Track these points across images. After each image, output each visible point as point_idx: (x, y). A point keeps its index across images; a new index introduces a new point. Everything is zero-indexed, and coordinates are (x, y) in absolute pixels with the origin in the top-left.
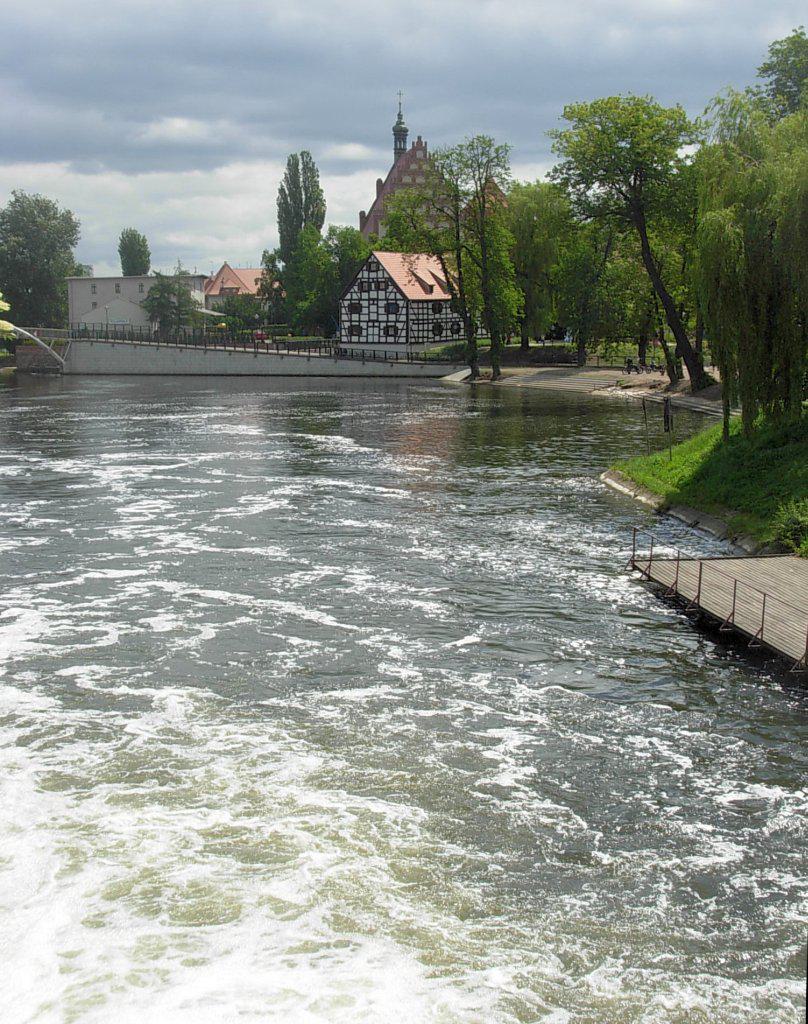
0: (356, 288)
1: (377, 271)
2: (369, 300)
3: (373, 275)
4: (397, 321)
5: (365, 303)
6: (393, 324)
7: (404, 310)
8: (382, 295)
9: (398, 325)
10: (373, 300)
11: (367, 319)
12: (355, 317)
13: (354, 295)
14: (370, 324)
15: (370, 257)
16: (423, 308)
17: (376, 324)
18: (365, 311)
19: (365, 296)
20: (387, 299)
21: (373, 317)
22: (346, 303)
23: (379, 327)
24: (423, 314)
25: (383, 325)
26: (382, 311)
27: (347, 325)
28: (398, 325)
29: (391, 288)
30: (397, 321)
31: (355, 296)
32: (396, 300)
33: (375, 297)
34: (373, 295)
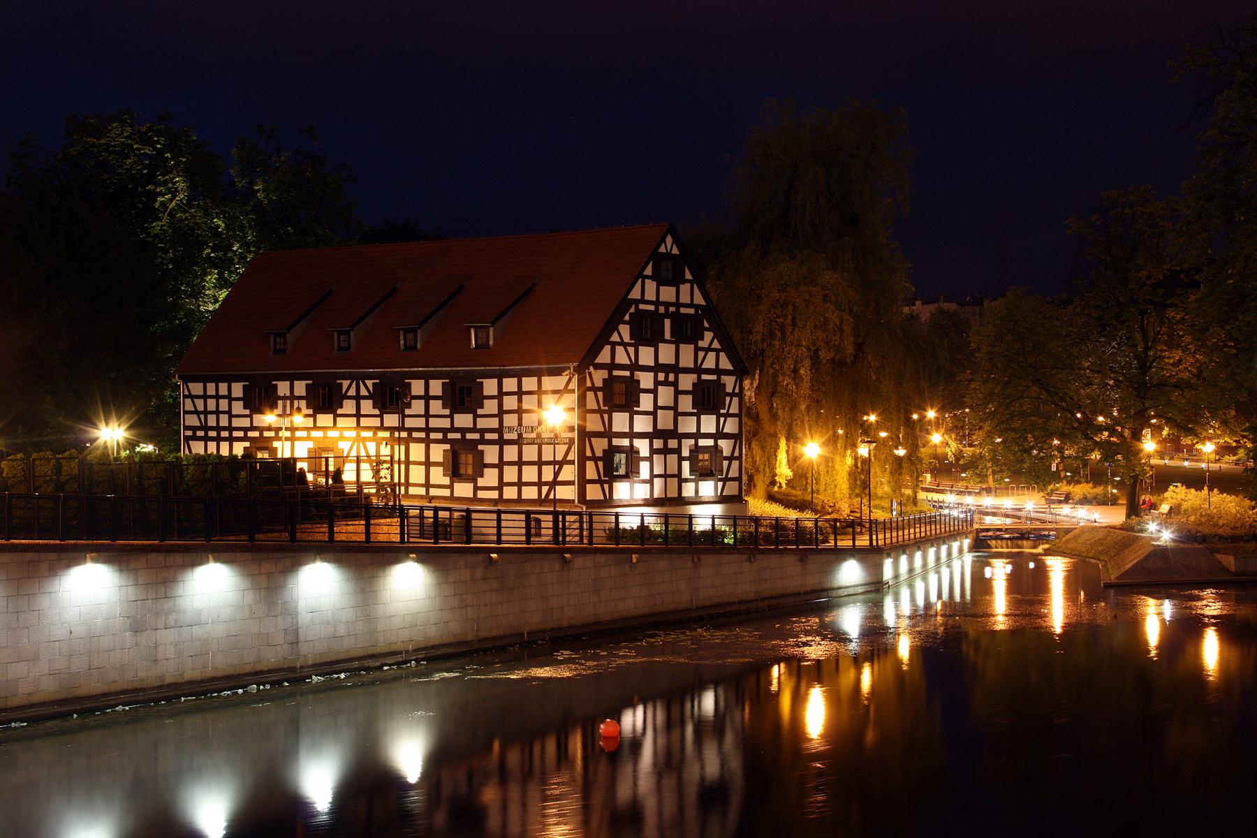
0: (625, 331)
1: (676, 281)
2: (657, 368)
3: (668, 294)
4: (719, 435)
5: (646, 380)
6: (710, 442)
7: (735, 400)
8: (687, 356)
9: (723, 443)
10: (667, 369)
11: (650, 430)
12: (620, 421)
13: (620, 350)
14: (658, 444)
15: (663, 240)
16: (217, 397)
17: (673, 444)
18: (646, 402)
19: (646, 356)
20: (697, 370)
21: (665, 419)
22: (599, 377)
23: (678, 451)
24: (217, 412)
25: (687, 444)
26: (686, 403)
27: (600, 445)
28: (721, 443)
29: (708, 336)
30: (719, 435)
31: (622, 357)
32: (718, 371)
33: (674, 363)
34: (667, 354)
